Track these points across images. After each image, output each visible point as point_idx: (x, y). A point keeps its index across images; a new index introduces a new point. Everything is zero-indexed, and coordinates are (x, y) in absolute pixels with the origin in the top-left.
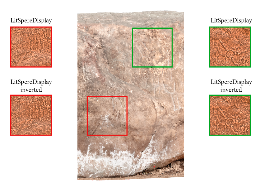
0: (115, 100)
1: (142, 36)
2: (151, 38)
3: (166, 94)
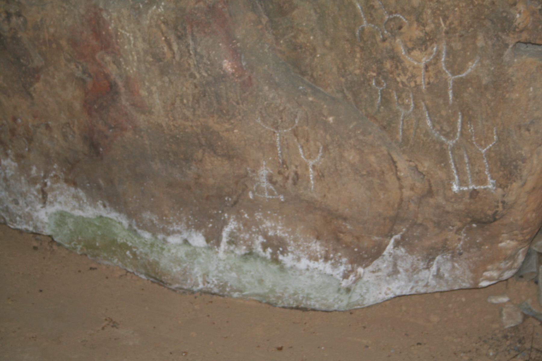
0: (285, 137)
3: (434, 141)
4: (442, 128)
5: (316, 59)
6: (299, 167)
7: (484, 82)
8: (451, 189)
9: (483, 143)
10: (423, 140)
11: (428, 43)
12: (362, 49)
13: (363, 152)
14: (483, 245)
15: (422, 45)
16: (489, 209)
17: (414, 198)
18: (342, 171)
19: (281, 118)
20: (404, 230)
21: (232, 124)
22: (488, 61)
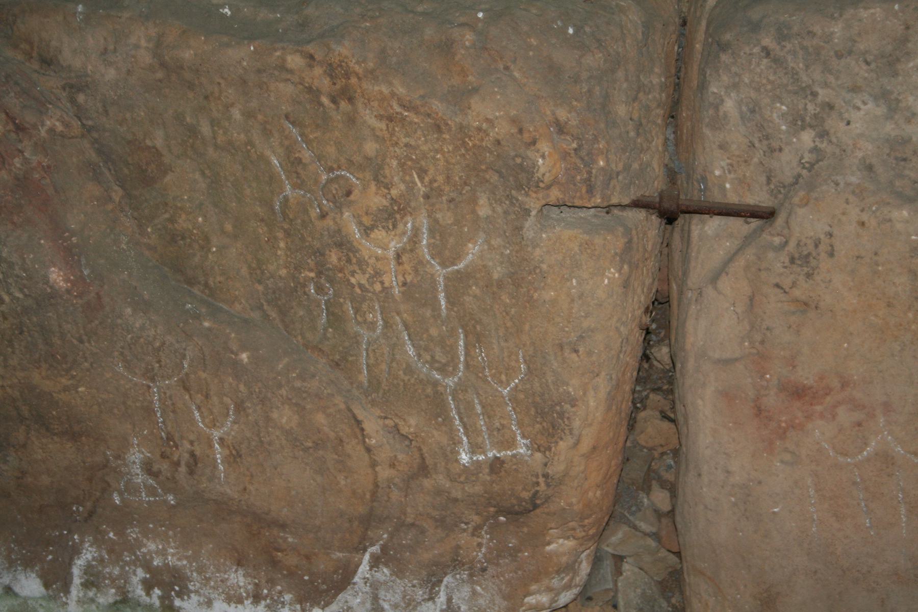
1: (281, 86)
2: (325, 100)
3: (421, 381)
4: (433, 357)
5: (210, 256)
6: (196, 444)
7: (496, 276)
8: (457, 461)
9: (503, 377)
10: (404, 381)
11: (398, 216)
12: (288, 233)
13: (304, 408)
14: (520, 551)
15: (387, 220)
16: (524, 489)
17: (397, 480)
18: (270, 444)
19: (159, 362)
20: (385, 536)
21: (73, 377)
22: (498, 240)
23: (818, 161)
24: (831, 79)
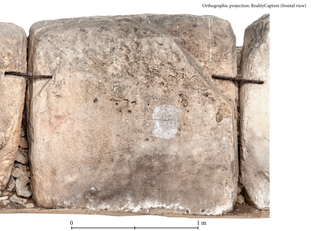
23: (60, 64)
24: (62, 46)
